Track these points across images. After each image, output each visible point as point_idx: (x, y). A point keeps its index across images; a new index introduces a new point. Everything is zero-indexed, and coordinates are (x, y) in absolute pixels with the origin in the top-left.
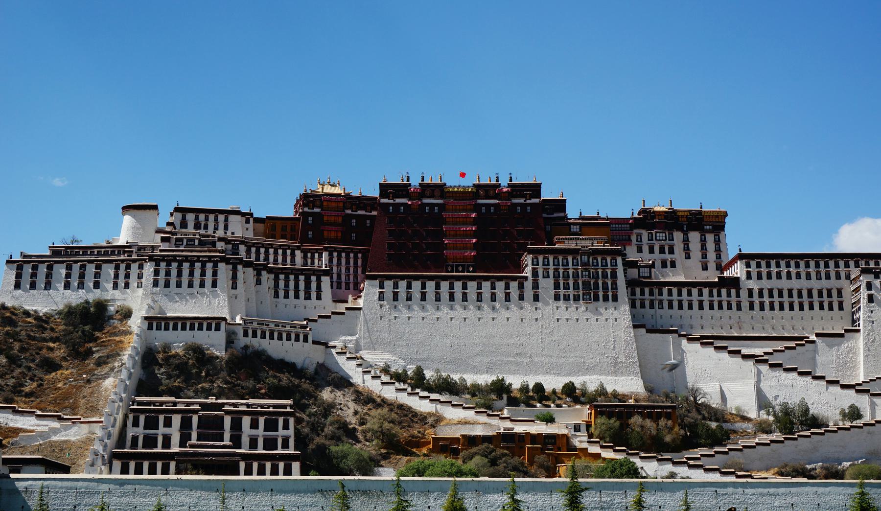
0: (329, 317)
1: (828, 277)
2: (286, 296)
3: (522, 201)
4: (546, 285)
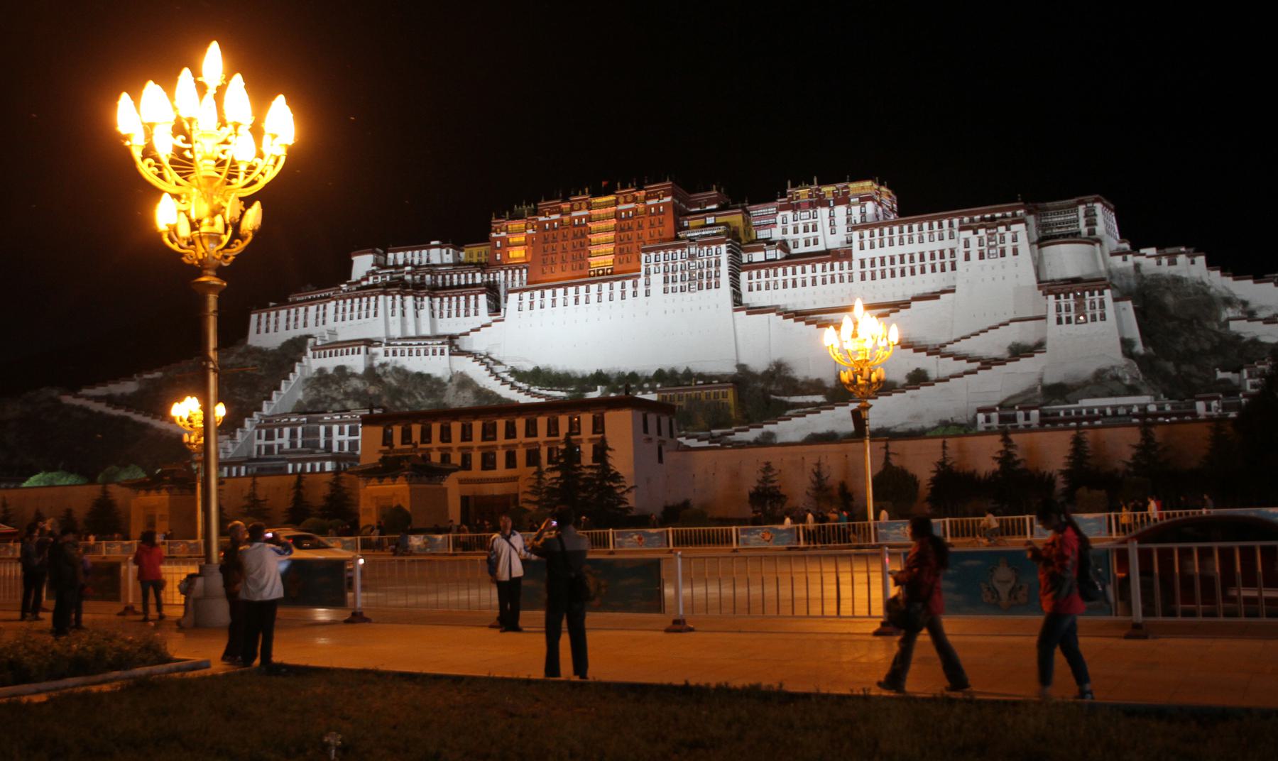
0: (477, 330)
1: (941, 238)
2: (449, 316)
3: (655, 201)
4: (657, 279)
